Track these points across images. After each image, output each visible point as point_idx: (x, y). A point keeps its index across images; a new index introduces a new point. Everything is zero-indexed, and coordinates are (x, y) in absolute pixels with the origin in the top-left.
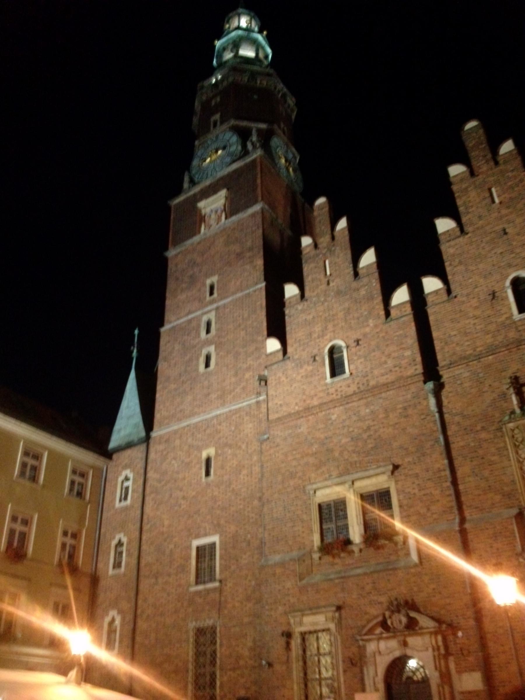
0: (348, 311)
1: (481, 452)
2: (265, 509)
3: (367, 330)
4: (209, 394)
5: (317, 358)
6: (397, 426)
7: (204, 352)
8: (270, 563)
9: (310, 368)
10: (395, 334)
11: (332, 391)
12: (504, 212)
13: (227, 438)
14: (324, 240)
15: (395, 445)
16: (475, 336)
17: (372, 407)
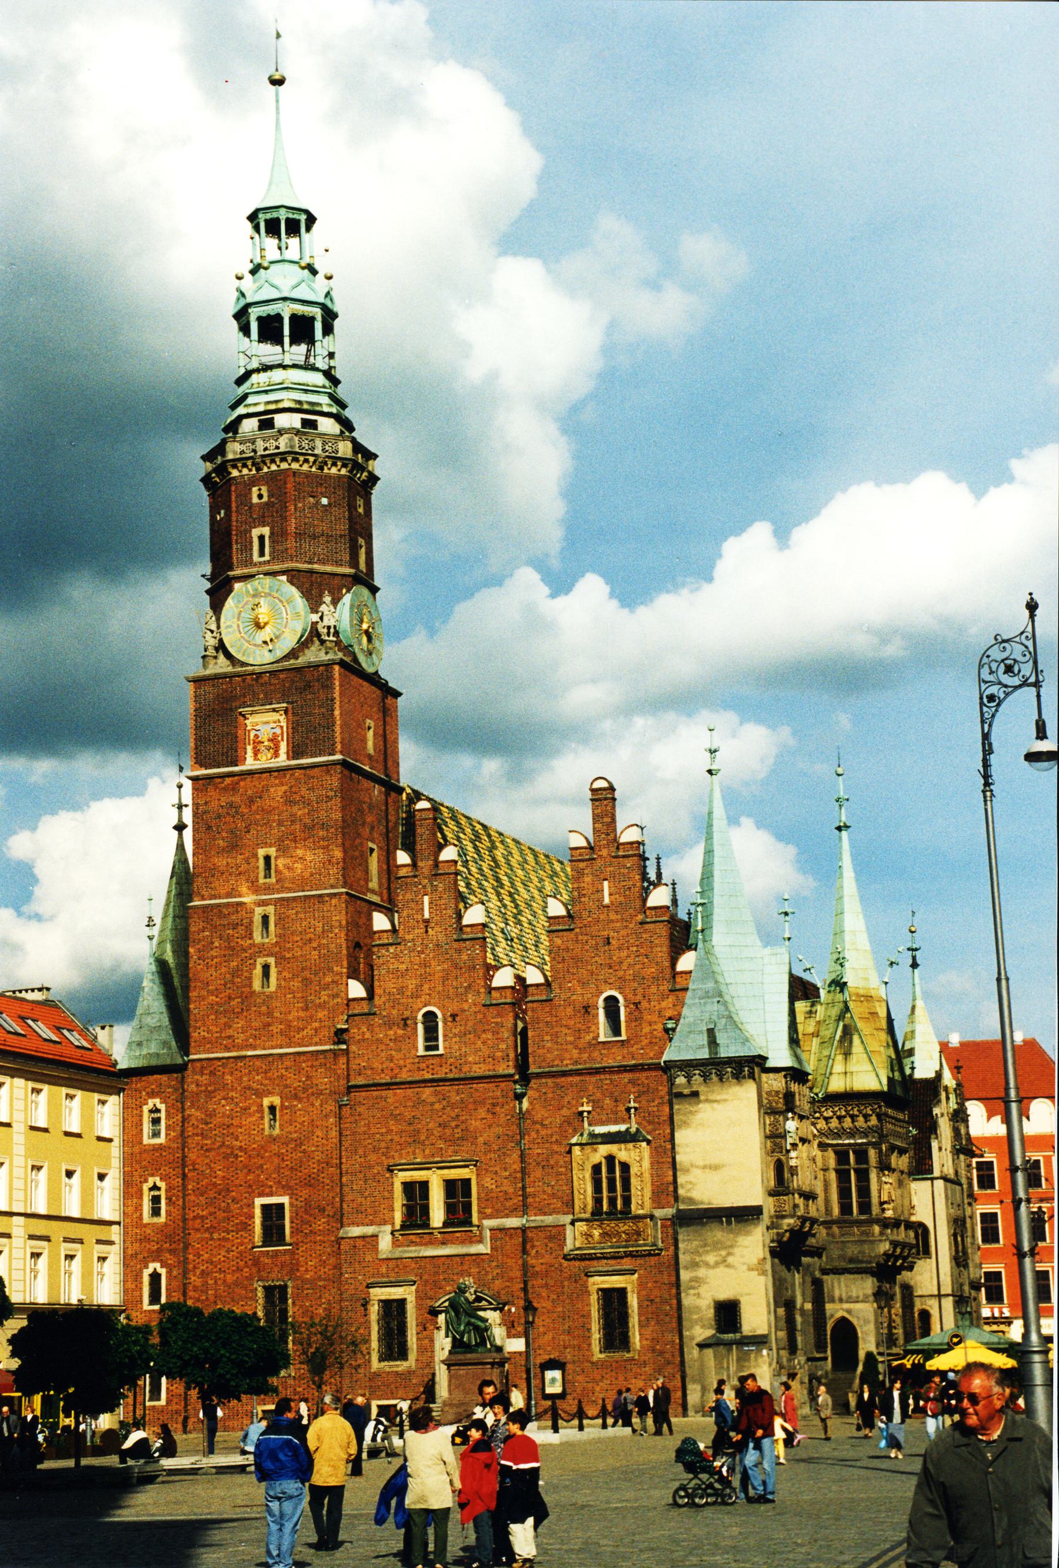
2: (344, 1179)
3: (466, 1007)
4: (269, 1025)
5: (409, 1022)
7: (260, 961)
8: (350, 1235)
9: (400, 1032)
11: (423, 1066)
12: (613, 916)
14: (425, 865)
15: (481, 1140)
16: (564, 1047)
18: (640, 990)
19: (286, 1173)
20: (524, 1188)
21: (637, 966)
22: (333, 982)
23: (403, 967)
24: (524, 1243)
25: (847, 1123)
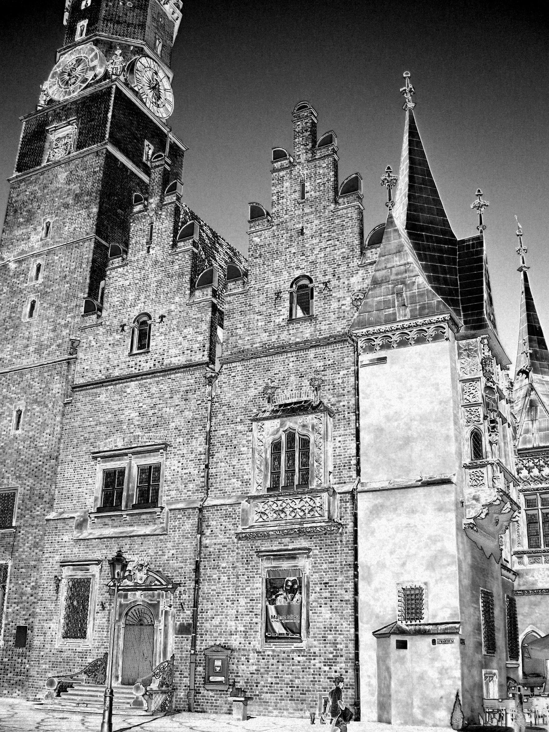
0: (160, 283)
1: (235, 442)
3: (173, 307)
4: (27, 346)
5: (126, 328)
6: (177, 408)
9: (118, 337)
10: (195, 317)
11: (132, 364)
13: (37, 395)
15: (173, 425)
16: (255, 332)
17: (161, 386)
18: (330, 270)
19: (20, 465)
20: (207, 466)
21: (328, 249)
22: (76, 306)
23: (127, 283)
24: (201, 521)
25: (535, 472)
